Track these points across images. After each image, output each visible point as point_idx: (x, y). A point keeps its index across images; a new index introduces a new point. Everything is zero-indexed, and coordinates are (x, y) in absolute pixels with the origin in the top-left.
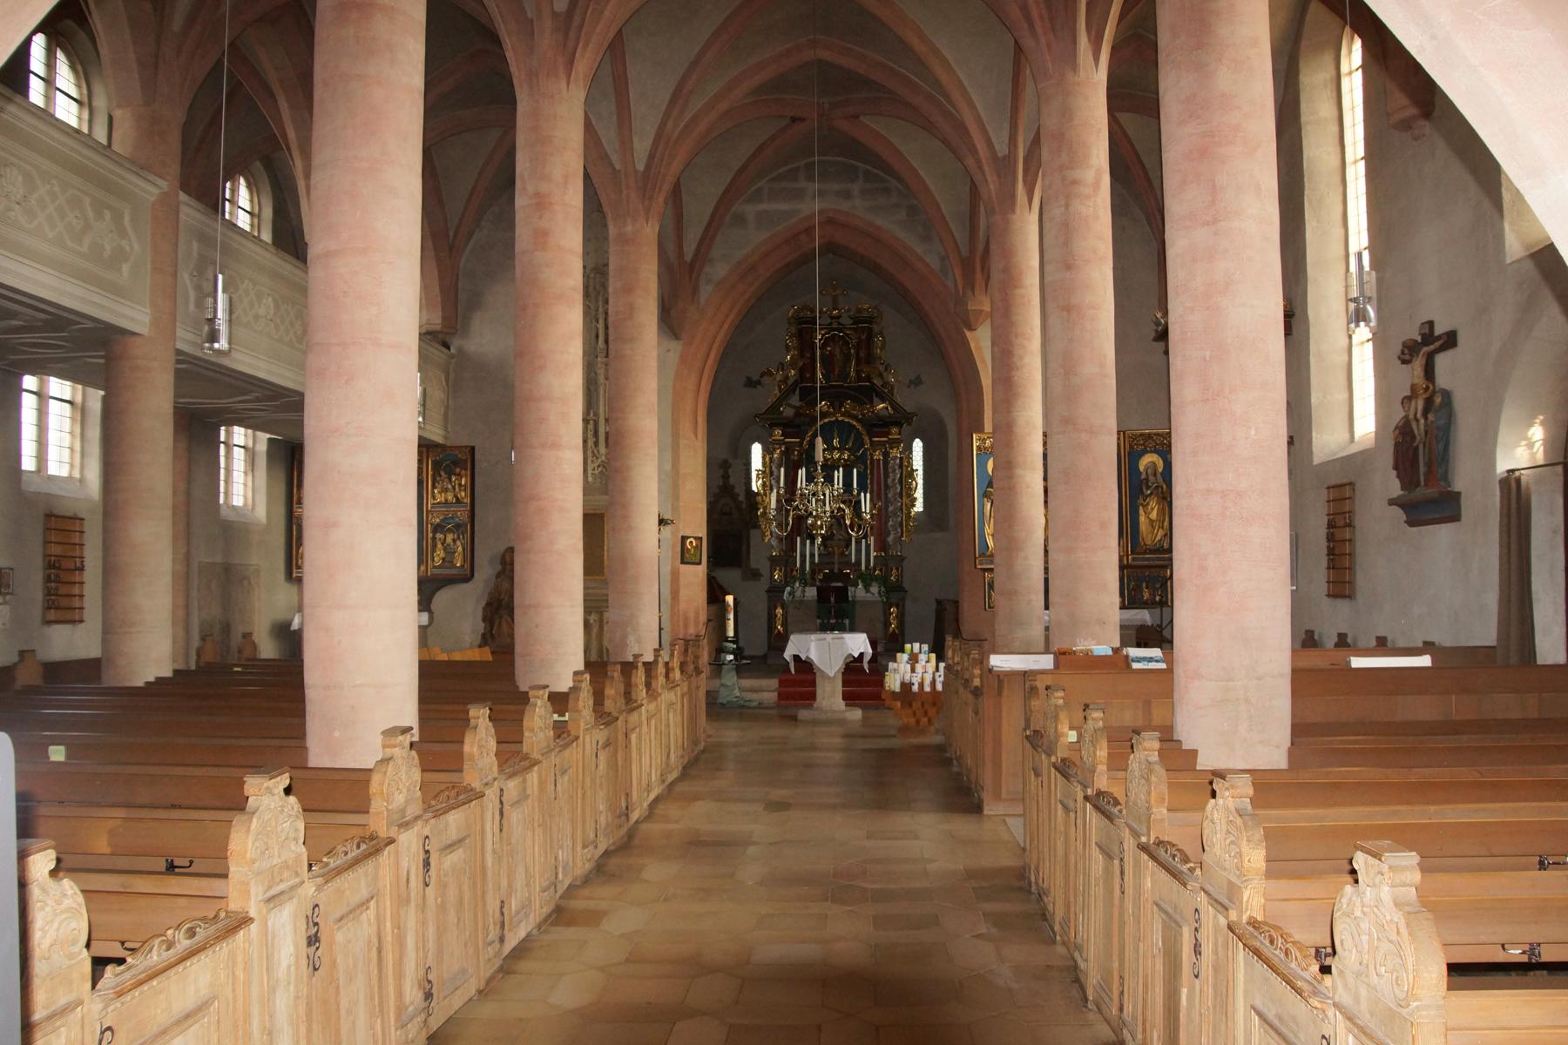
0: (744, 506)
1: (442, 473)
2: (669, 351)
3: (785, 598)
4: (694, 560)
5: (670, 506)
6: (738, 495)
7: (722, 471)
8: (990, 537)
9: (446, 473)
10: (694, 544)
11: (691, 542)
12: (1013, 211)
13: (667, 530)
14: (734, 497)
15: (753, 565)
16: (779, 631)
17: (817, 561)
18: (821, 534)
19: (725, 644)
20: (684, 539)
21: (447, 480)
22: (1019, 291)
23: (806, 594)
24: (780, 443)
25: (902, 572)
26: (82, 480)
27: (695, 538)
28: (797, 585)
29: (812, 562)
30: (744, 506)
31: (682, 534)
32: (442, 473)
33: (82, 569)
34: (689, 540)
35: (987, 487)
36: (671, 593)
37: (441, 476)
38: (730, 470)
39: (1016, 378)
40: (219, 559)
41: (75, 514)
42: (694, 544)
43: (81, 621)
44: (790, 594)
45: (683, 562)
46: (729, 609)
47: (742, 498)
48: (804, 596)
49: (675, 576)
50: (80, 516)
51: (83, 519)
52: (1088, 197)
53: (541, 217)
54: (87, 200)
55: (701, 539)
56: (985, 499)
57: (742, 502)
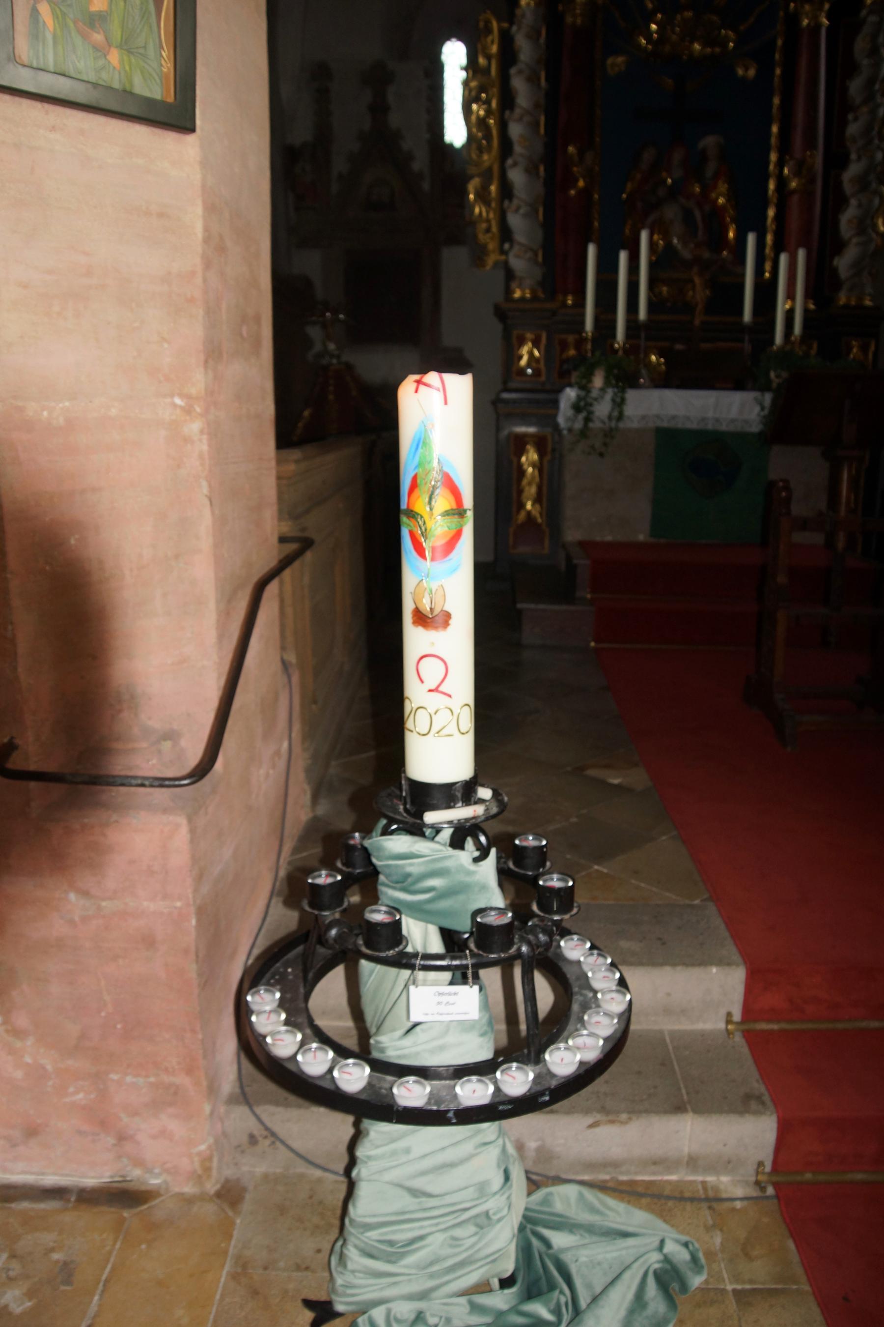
0: (426, 186)
3: (561, 420)
17: (642, 314)
25: (875, 354)
28: (598, 381)
29: (632, 323)
30: (426, 186)
44: (577, 408)
48: (620, 417)
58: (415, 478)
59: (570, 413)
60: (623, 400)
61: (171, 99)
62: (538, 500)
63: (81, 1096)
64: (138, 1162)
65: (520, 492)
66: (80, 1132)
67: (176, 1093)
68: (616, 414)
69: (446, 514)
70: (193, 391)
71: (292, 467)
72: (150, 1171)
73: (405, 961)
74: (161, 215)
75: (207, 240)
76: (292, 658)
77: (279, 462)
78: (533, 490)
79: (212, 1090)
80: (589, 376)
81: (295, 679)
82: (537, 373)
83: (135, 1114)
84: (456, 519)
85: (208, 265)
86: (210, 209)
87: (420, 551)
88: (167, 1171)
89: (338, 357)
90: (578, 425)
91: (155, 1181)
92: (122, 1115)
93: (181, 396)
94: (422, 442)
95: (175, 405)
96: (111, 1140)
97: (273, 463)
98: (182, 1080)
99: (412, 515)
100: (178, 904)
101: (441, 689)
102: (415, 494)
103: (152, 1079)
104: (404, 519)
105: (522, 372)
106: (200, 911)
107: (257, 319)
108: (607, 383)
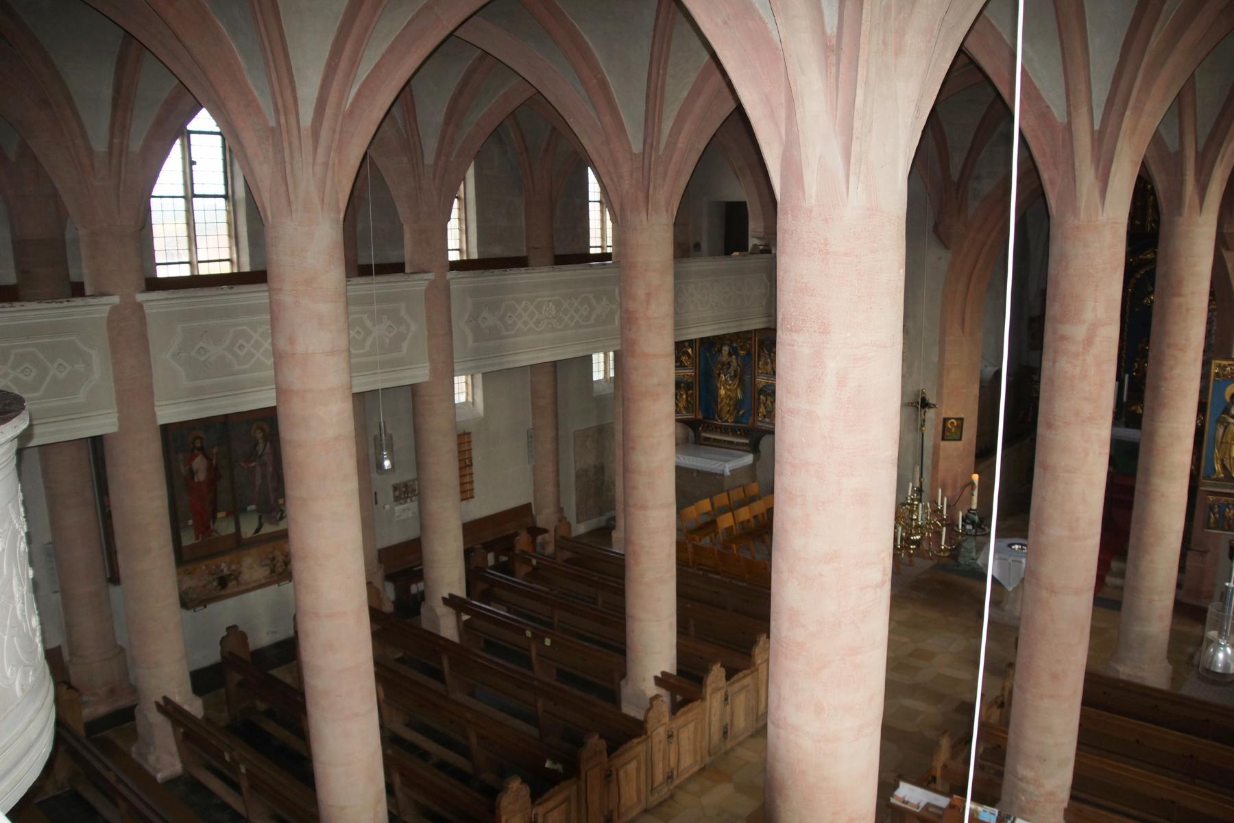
1: (765, 350)
2: (940, 259)
4: (955, 437)
5: (935, 391)
8: (1219, 462)
9: (767, 351)
10: (955, 424)
12: (1180, 215)
13: (930, 414)
18: (901, 554)
20: (945, 420)
21: (768, 356)
22: (1177, 300)
26: (473, 403)
27: (956, 419)
31: (944, 416)
32: (765, 350)
33: (471, 465)
35: (1223, 413)
37: (764, 352)
39: (1163, 389)
40: (593, 424)
41: (464, 431)
42: (955, 424)
43: (473, 497)
45: (943, 439)
49: (936, 450)
50: (467, 431)
51: (470, 433)
52: (1076, 355)
53: (630, 330)
54: (365, 317)
55: (961, 420)
56: (1218, 425)
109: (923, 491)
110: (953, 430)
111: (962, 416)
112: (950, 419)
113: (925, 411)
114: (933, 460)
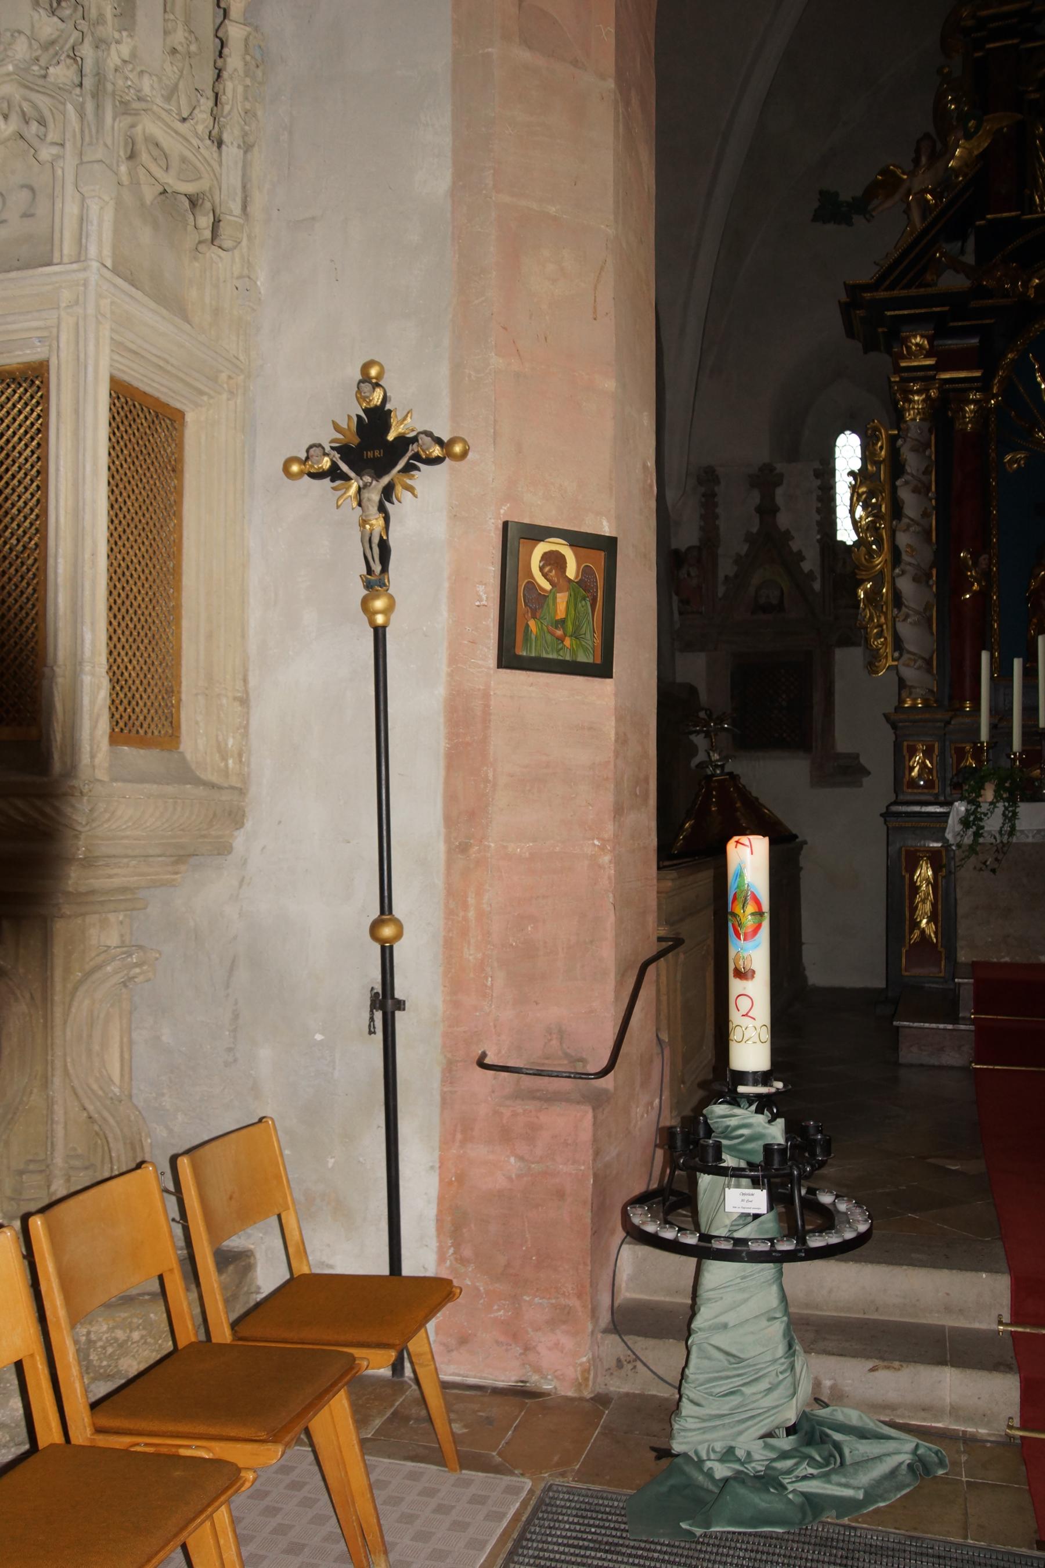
5: (444, 370)
6: (800, 557)
7: (755, 498)
10: (571, 571)
11: (553, 560)
14: (790, 562)
15: (843, 744)
16: (923, 931)
19: (719, 1110)
23: (1021, 825)
24: (925, 376)
27: (578, 540)
30: (817, 586)
34: (541, 548)
36: (449, 821)
38: (779, 492)
42: (571, 571)
44: (965, 822)
46: (747, 916)
47: (810, 563)
48: (1012, 832)
55: (608, 546)
57: (811, 575)
58: (735, 894)
59: (959, 828)
60: (1015, 814)
61: (598, 661)
62: (933, 918)
63: (502, 1313)
64: (537, 1370)
65: (914, 909)
66: (497, 1342)
67: (569, 1313)
68: (1007, 828)
69: (752, 914)
70: (606, 836)
71: (669, 884)
72: (545, 1377)
73: (723, 1172)
74: (590, 728)
75: (616, 741)
76: (665, 1037)
77: (659, 880)
78: (928, 907)
79: (594, 1314)
80: (979, 788)
81: (667, 1052)
82: (930, 784)
83: (537, 1329)
84: (758, 917)
85: (617, 755)
86: (620, 719)
87: (738, 936)
88: (557, 1377)
89: (722, 767)
90: (968, 840)
91: (547, 1387)
92: (530, 1330)
93: (598, 839)
94: (740, 875)
95: (594, 845)
96: (519, 1350)
97: (655, 881)
98: (574, 1302)
99: (734, 915)
100: (583, 1168)
101: (749, 1014)
102: (736, 902)
103: (553, 1301)
104: (730, 917)
105: (913, 783)
106: (596, 1176)
107: (646, 780)
108: (998, 796)
109: (400, 1005)
110: (562, 600)
111: (606, 529)
112: (537, 533)
113: (388, 492)
114: (451, 798)
